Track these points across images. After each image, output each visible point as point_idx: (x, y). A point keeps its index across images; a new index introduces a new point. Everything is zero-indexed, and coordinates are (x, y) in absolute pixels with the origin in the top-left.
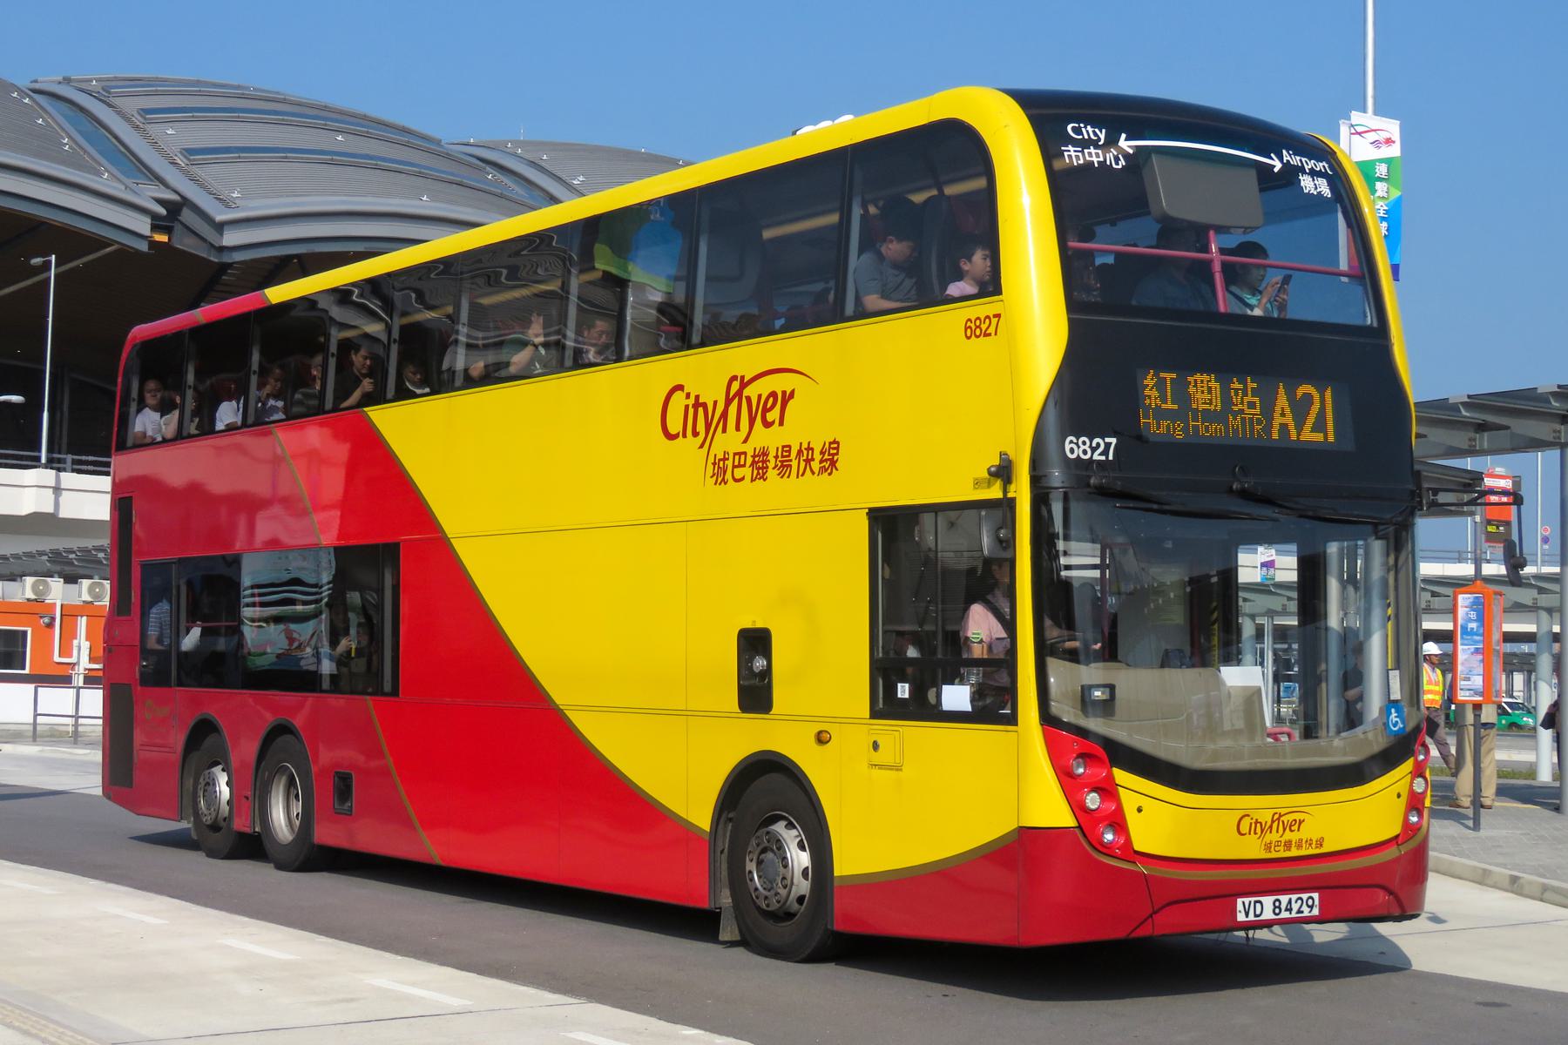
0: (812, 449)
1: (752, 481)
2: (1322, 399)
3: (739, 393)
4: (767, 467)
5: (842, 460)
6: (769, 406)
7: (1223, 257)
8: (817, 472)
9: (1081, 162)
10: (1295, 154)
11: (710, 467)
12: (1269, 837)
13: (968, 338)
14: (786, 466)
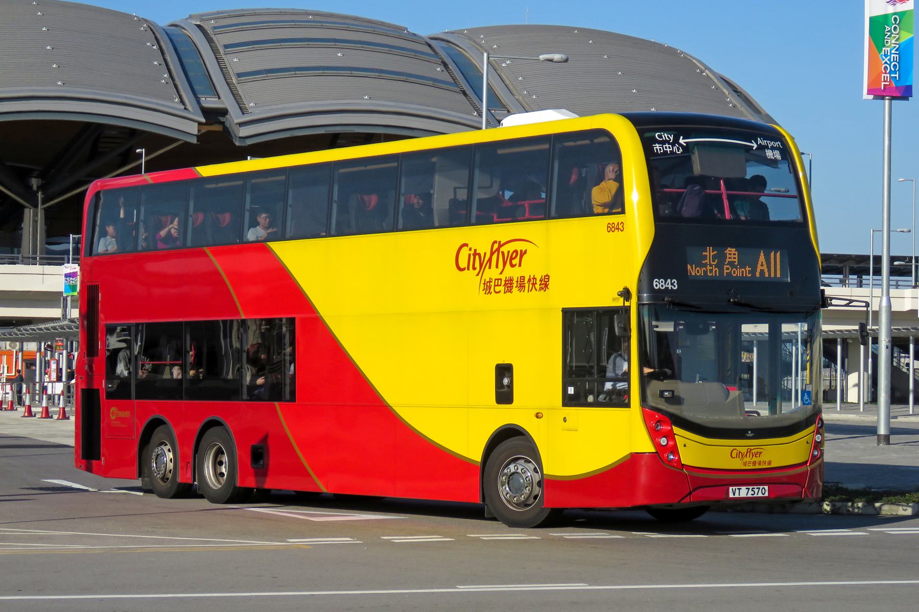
0: (536, 279)
1: (505, 293)
2: (776, 257)
3: (498, 250)
4: (512, 287)
5: (551, 283)
6: (513, 256)
7: (728, 192)
8: (538, 289)
9: (662, 151)
10: (764, 140)
11: (482, 286)
12: (745, 459)
13: (609, 232)
14: (523, 286)
